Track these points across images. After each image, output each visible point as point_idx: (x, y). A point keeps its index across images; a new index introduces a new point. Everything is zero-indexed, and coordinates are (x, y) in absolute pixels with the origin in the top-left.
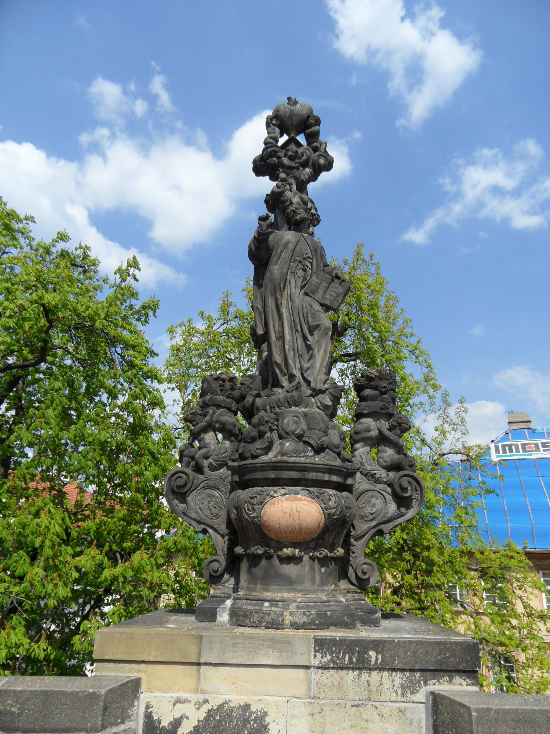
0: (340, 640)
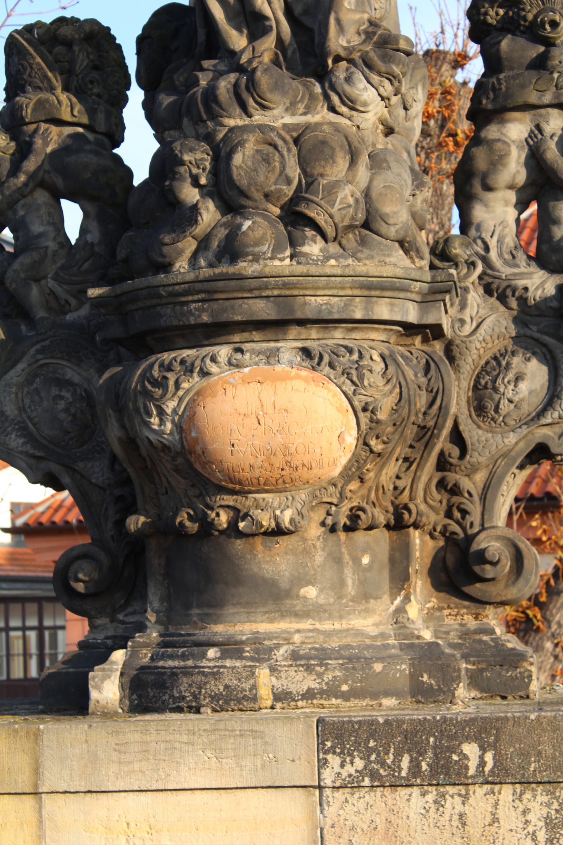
0: (387, 722)
